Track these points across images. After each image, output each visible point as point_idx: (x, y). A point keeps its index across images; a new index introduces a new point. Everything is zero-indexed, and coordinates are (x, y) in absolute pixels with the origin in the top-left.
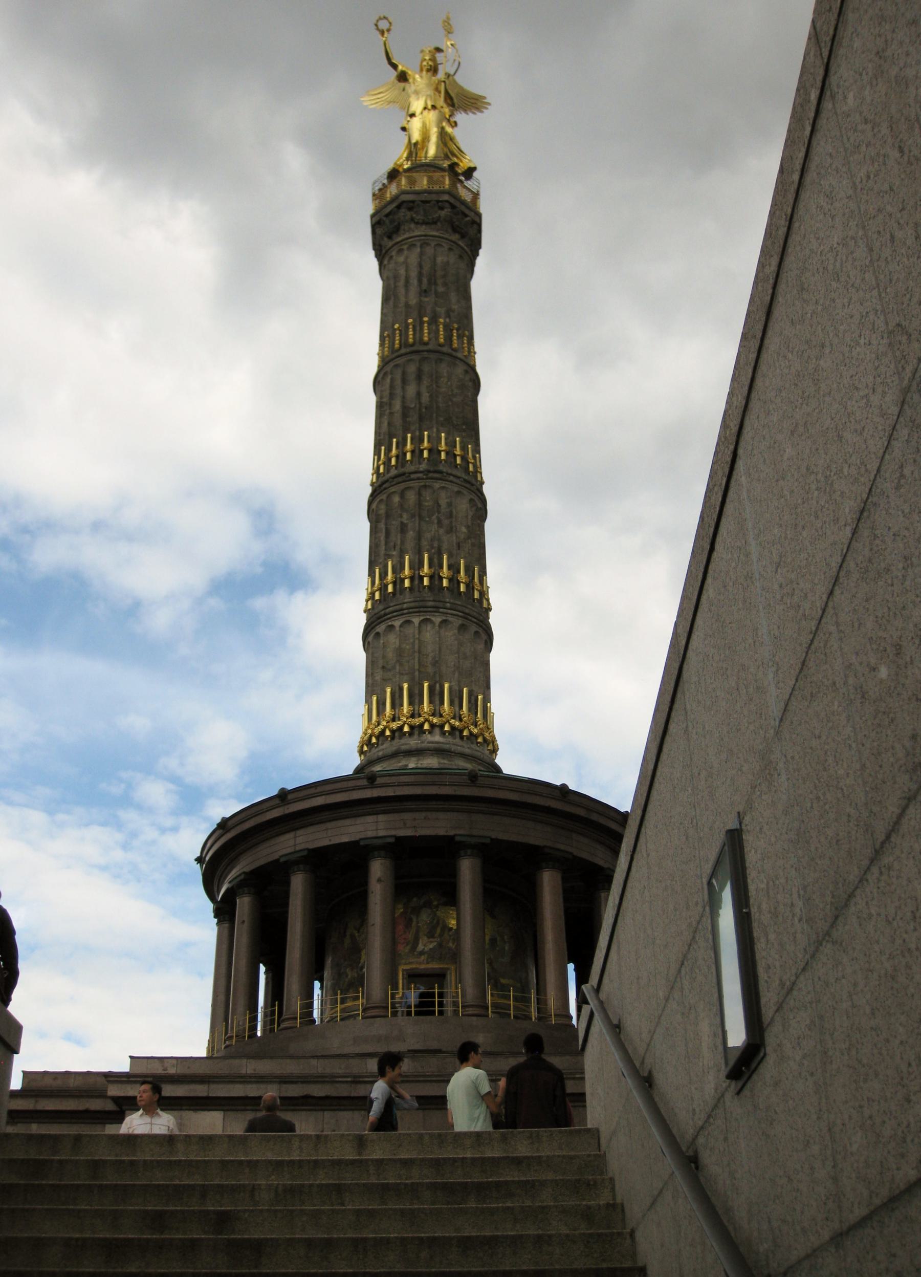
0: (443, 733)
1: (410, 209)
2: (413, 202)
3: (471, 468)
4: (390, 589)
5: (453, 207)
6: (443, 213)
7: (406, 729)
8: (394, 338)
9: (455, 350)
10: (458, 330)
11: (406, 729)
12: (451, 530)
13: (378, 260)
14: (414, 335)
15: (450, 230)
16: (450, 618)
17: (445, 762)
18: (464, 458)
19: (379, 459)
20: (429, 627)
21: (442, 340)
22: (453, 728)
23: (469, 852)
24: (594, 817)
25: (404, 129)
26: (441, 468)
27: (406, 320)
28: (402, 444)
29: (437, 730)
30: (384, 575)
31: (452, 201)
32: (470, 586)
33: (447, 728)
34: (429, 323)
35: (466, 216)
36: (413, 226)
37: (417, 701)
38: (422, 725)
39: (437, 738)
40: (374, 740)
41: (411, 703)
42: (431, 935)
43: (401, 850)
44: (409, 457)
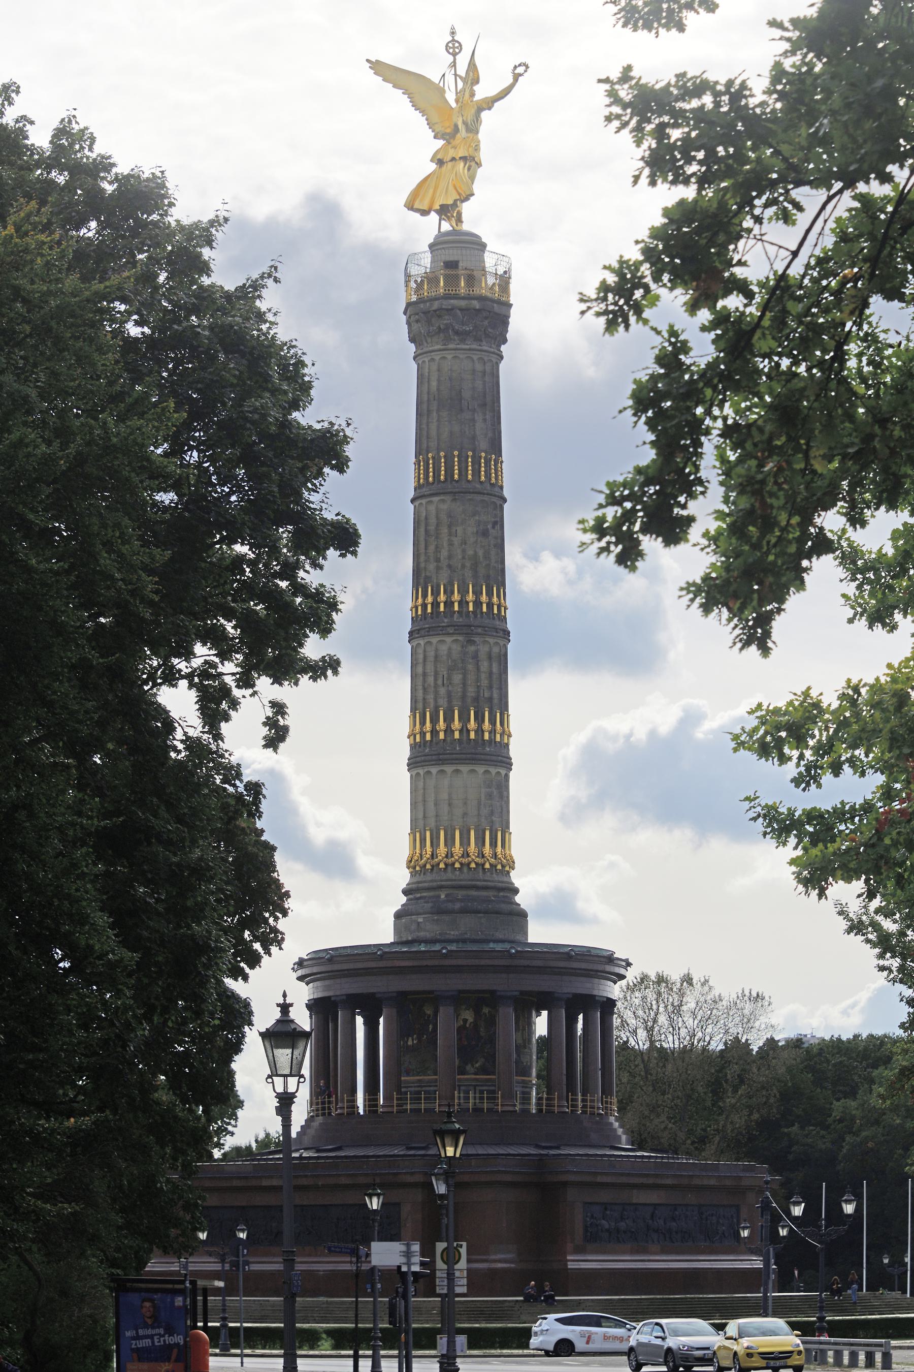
3: (496, 611)
4: (428, 737)
7: (442, 866)
8: (428, 468)
9: (481, 483)
10: (485, 458)
11: (442, 866)
18: (490, 605)
19: (417, 598)
22: (477, 864)
27: (438, 453)
28: (436, 593)
29: (465, 869)
30: (423, 723)
32: (493, 732)
37: (449, 843)
40: (418, 868)
41: (446, 845)
44: (442, 609)
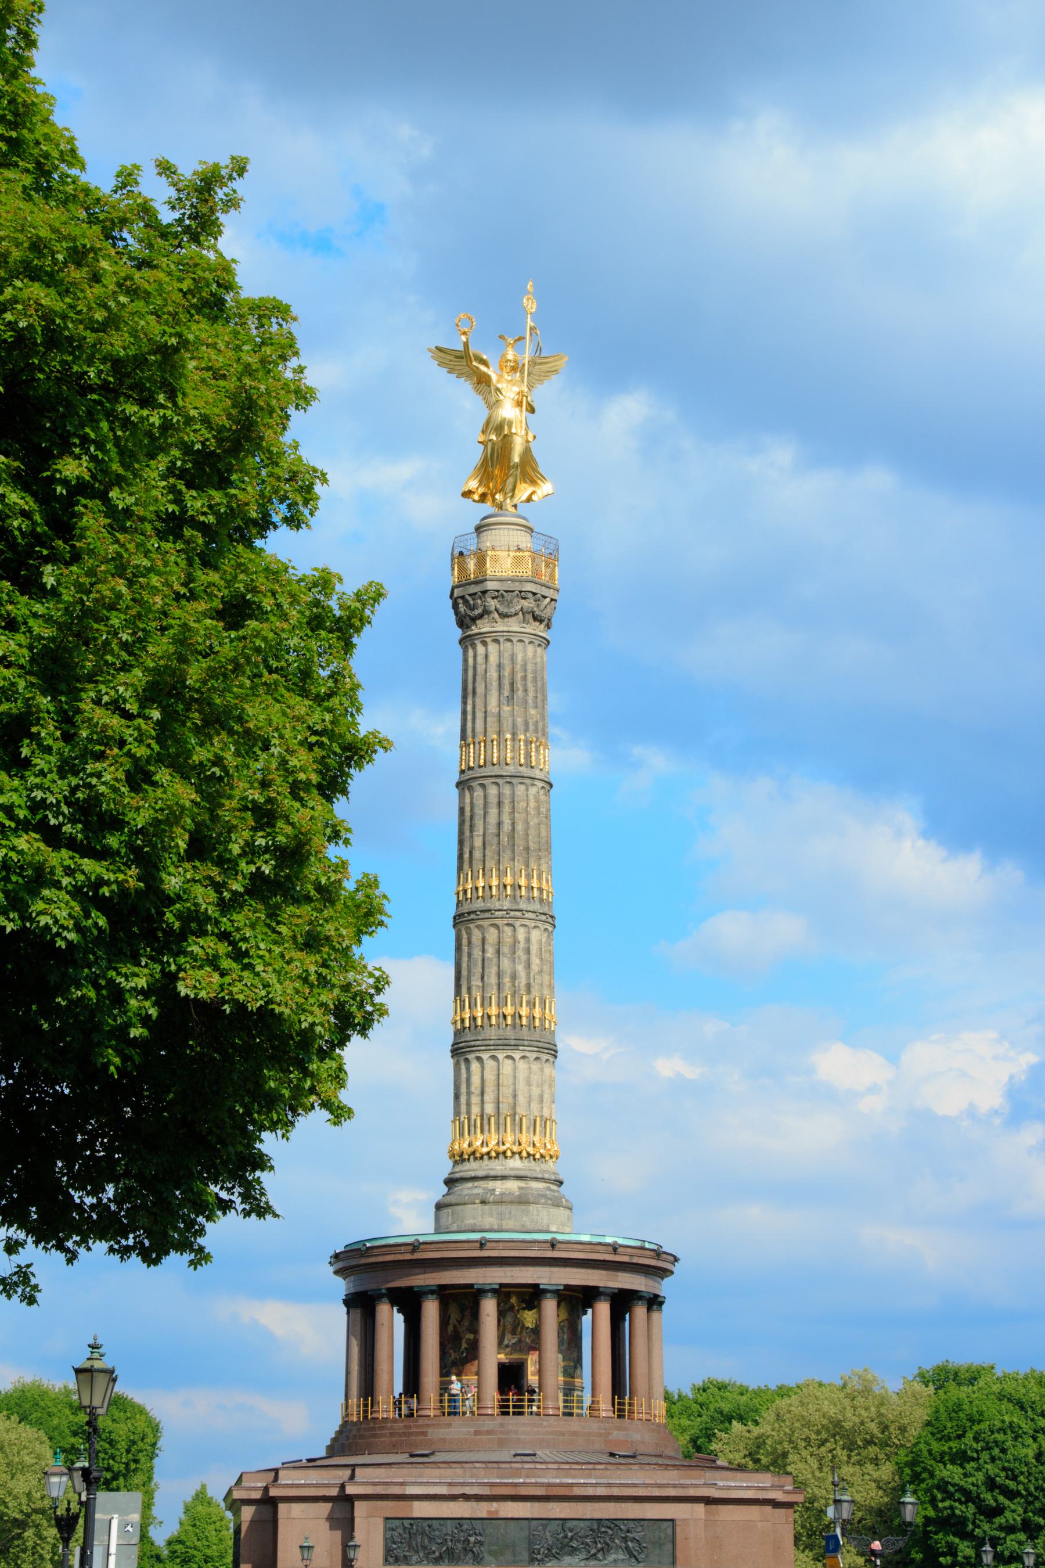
0: (521, 1158)
1: (493, 598)
2: (498, 591)
5: (534, 594)
6: (525, 603)
7: (493, 1154)
12: (528, 966)
14: (499, 751)
15: (531, 620)
16: (527, 1054)
17: (521, 1184)
18: (540, 889)
20: (510, 1061)
21: (522, 761)
22: (529, 1154)
23: (549, 1295)
24: (635, 1260)
26: (523, 906)
29: (517, 1156)
32: (543, 1019)
33: (524, 1154)
34: (513, 739)
35: (545, 597)
36: (496, 615)
38: (504, 1153)
39: (515, 1163)
42: (513, 1332)
43: (503, 1292)
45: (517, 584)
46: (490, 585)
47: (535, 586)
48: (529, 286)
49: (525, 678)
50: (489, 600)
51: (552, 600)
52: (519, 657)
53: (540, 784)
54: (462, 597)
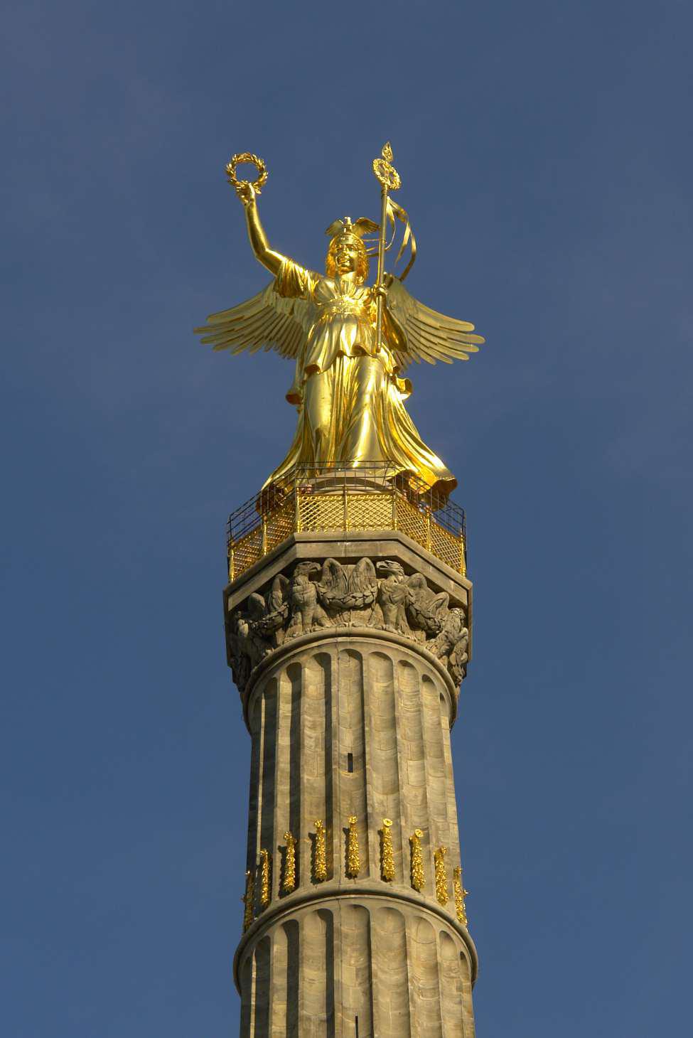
1: (315, 577)
2: (321, 560)
5: (409, 570)
13: (241, 689)
15: (404, 623)
25: (293, 398)
31: (406, 557)
35: (437, 589)
36: (320, 612)
45: (366, 545)
46: (302, 551)
47: (410, 554)
48: (387, 151)
49: (393, 723)
50: (302, 579)
51: (453, 604)
52: (377, 687)
53: (439, 926)
54: (247, 608)
